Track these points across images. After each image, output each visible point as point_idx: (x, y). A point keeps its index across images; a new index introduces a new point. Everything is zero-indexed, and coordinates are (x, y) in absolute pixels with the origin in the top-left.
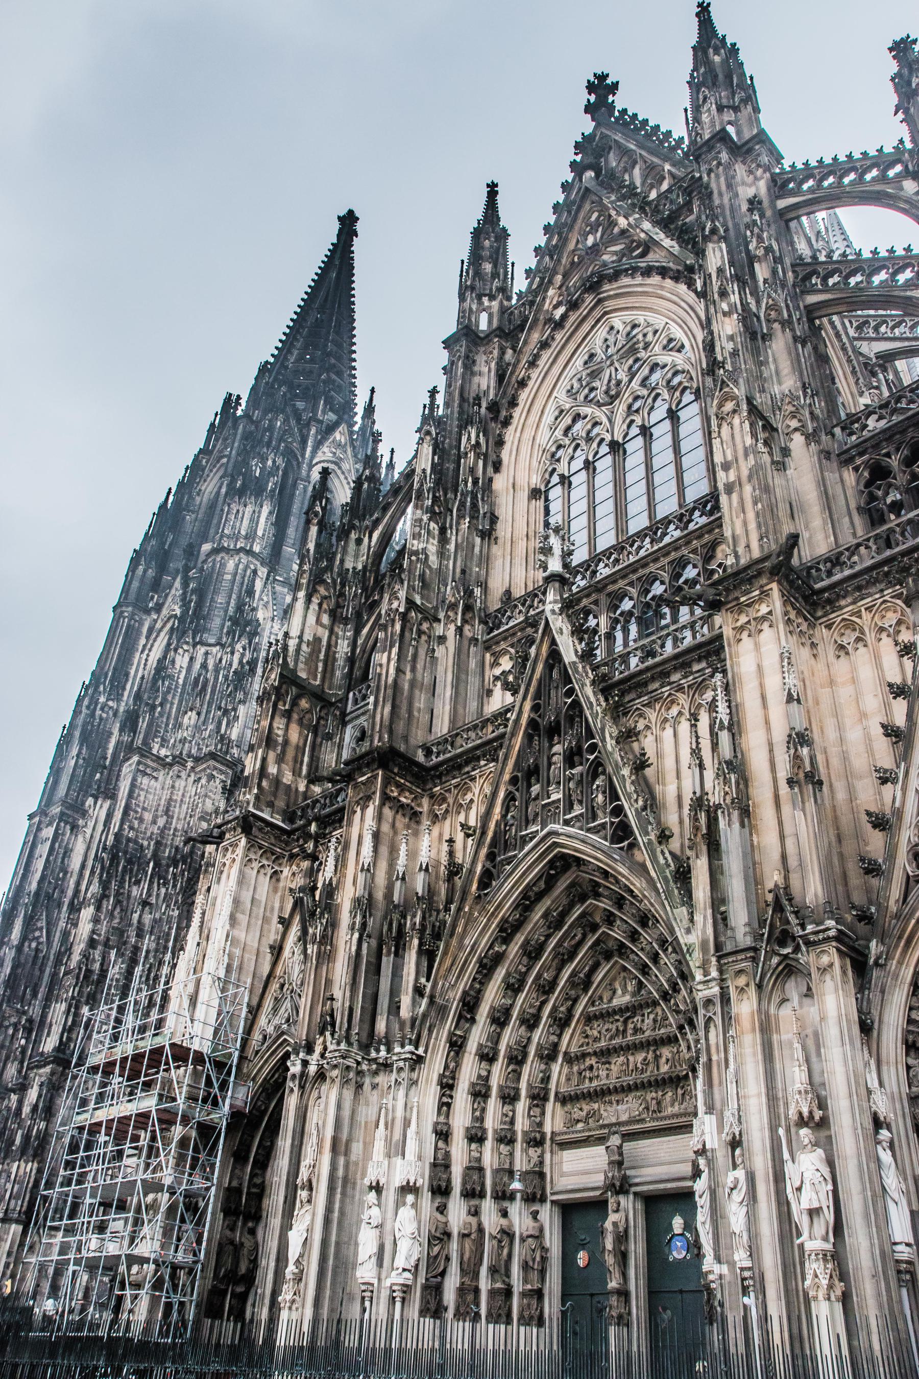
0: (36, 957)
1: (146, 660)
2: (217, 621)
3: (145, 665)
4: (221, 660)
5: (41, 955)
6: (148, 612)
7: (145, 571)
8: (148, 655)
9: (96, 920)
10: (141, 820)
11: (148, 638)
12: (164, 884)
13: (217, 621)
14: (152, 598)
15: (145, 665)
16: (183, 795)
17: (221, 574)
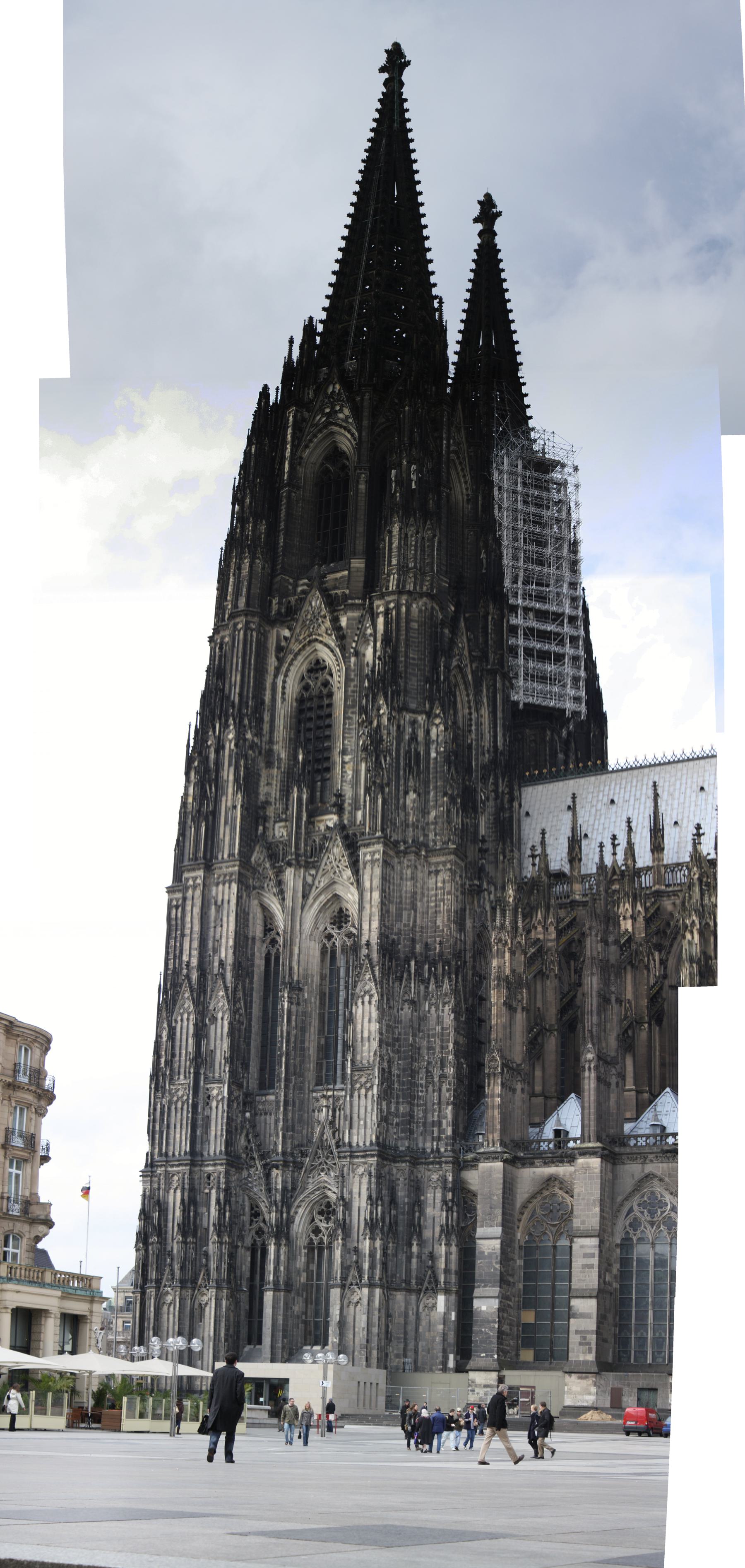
0: (240, 1030)
1: (284, 688)
2: (414, 683)
3: (283, 693)
4: (428, 732)
5: (243, 1027)
6: (273, 623)
7: (263, 568)
8: (284, 682)
9: (380, 1021)
10: (388, 911)
11: (280, 661)
12: (423, 981)
13: (414, 683)
14: (271, 602)
15: (283, 693)
16: (422, 888)
17: (408, 620)
